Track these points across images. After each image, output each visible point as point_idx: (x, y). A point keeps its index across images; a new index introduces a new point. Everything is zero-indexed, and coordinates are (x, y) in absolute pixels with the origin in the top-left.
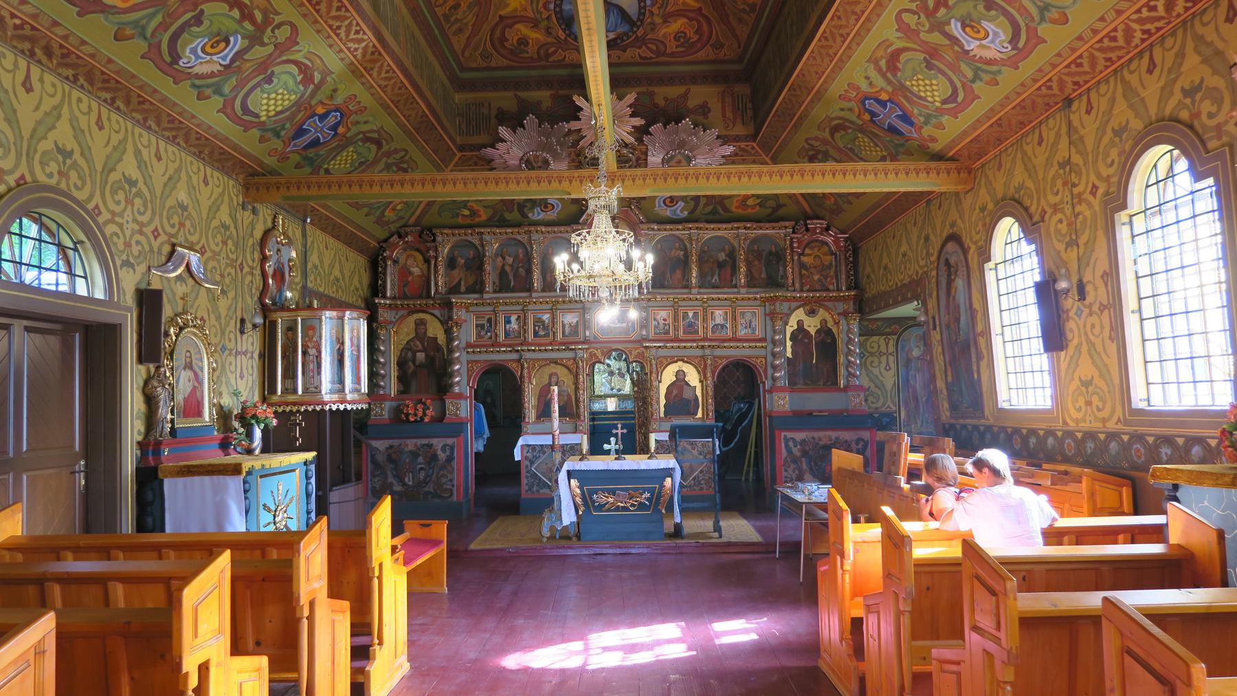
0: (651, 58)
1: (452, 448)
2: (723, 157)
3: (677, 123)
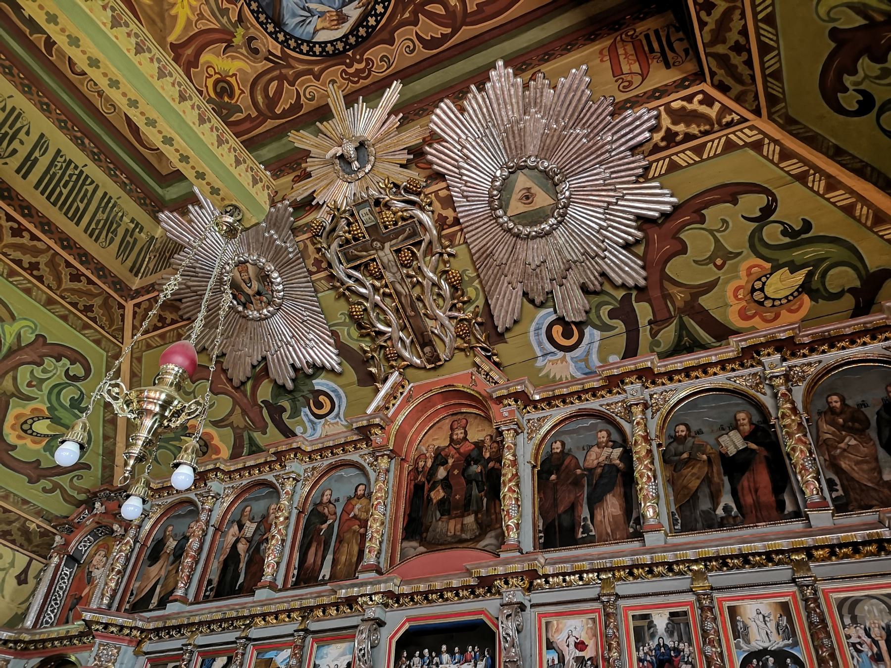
0: (445, 38)
3: (480, 88)
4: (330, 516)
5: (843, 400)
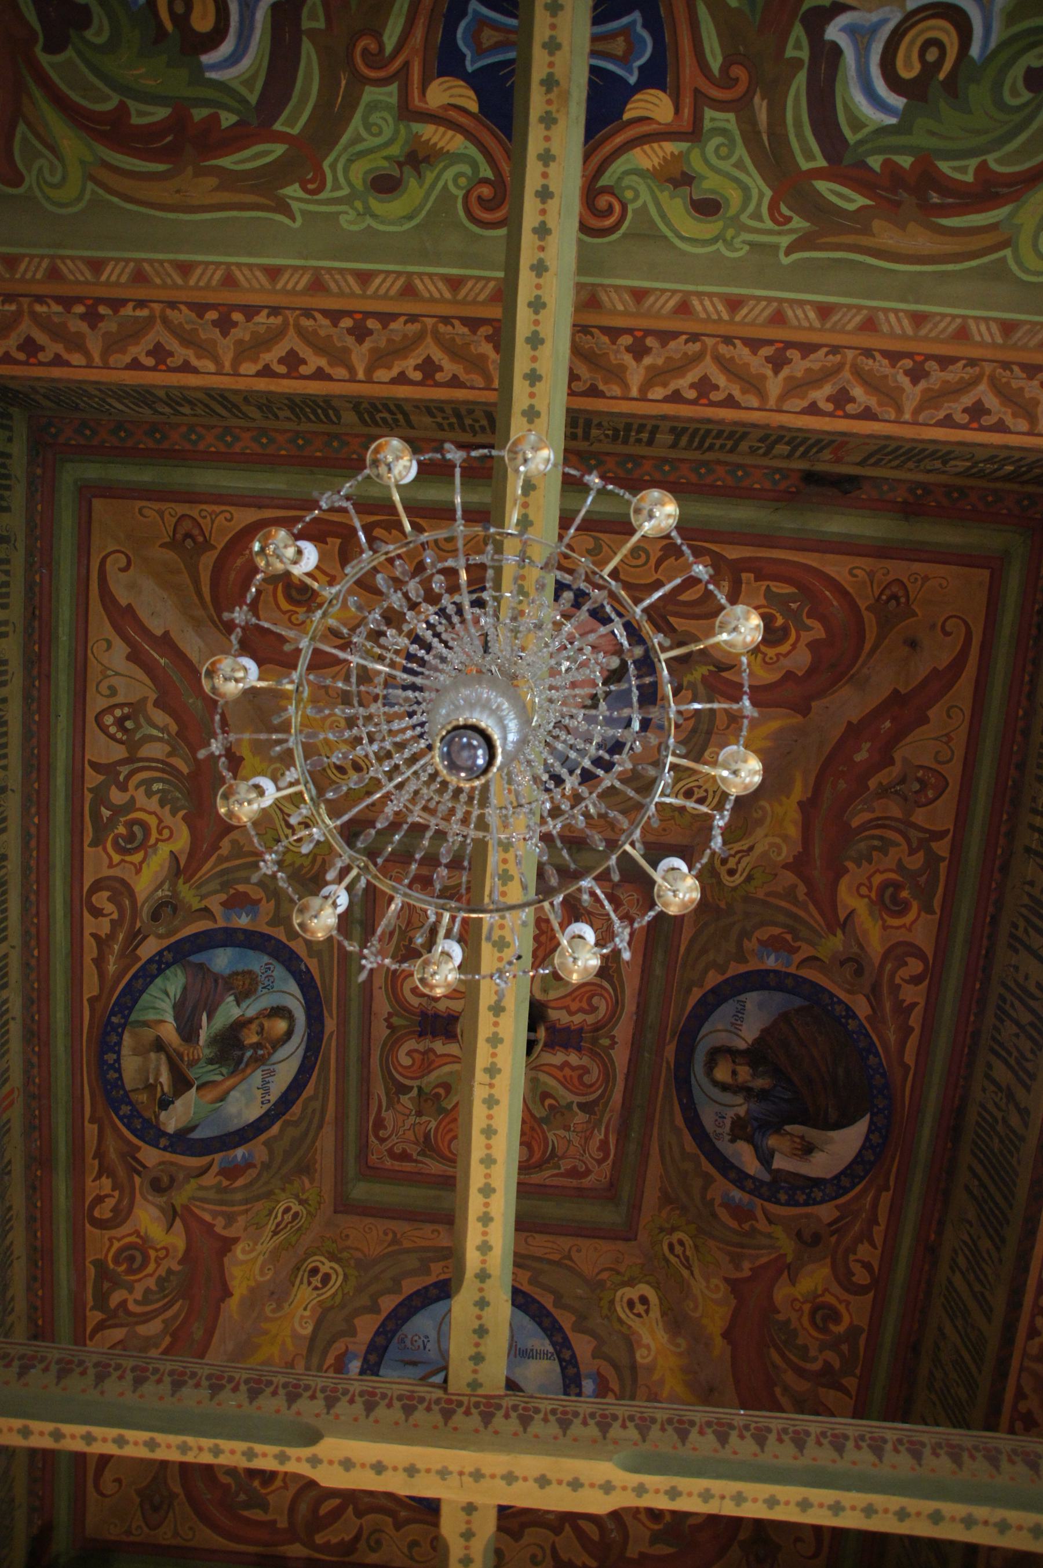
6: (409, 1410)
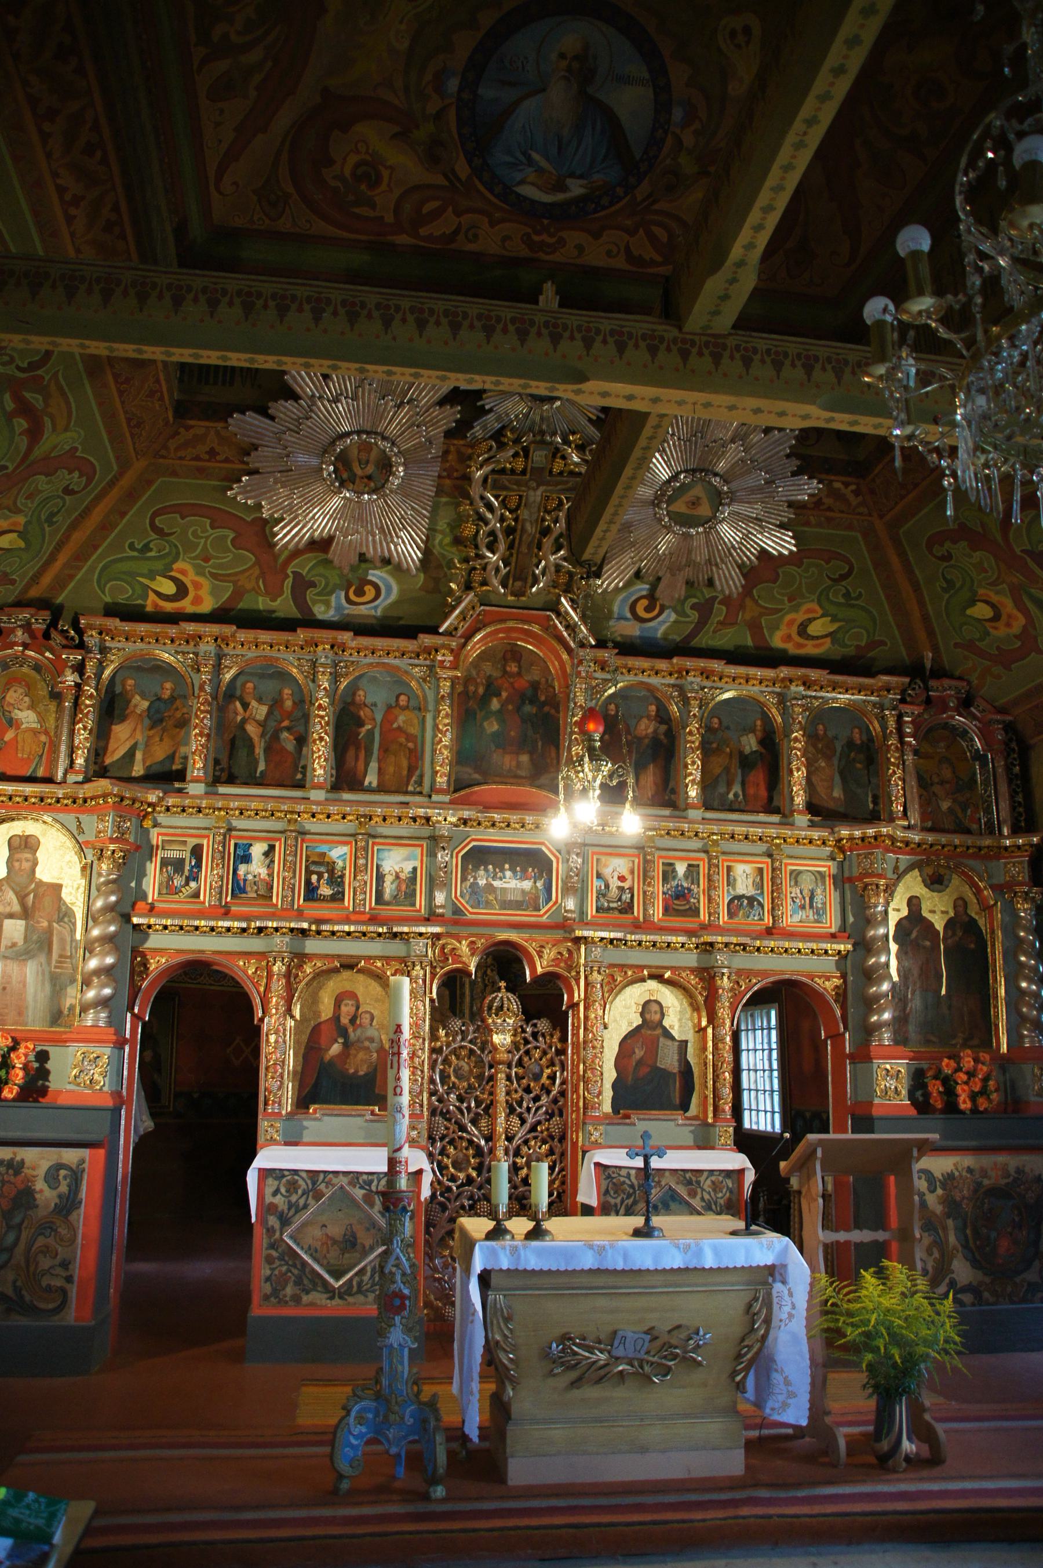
1: (76, 1175)
2: (791, 504)
4: (367, 721)
5: (825, 730)
6: (653, 350)
